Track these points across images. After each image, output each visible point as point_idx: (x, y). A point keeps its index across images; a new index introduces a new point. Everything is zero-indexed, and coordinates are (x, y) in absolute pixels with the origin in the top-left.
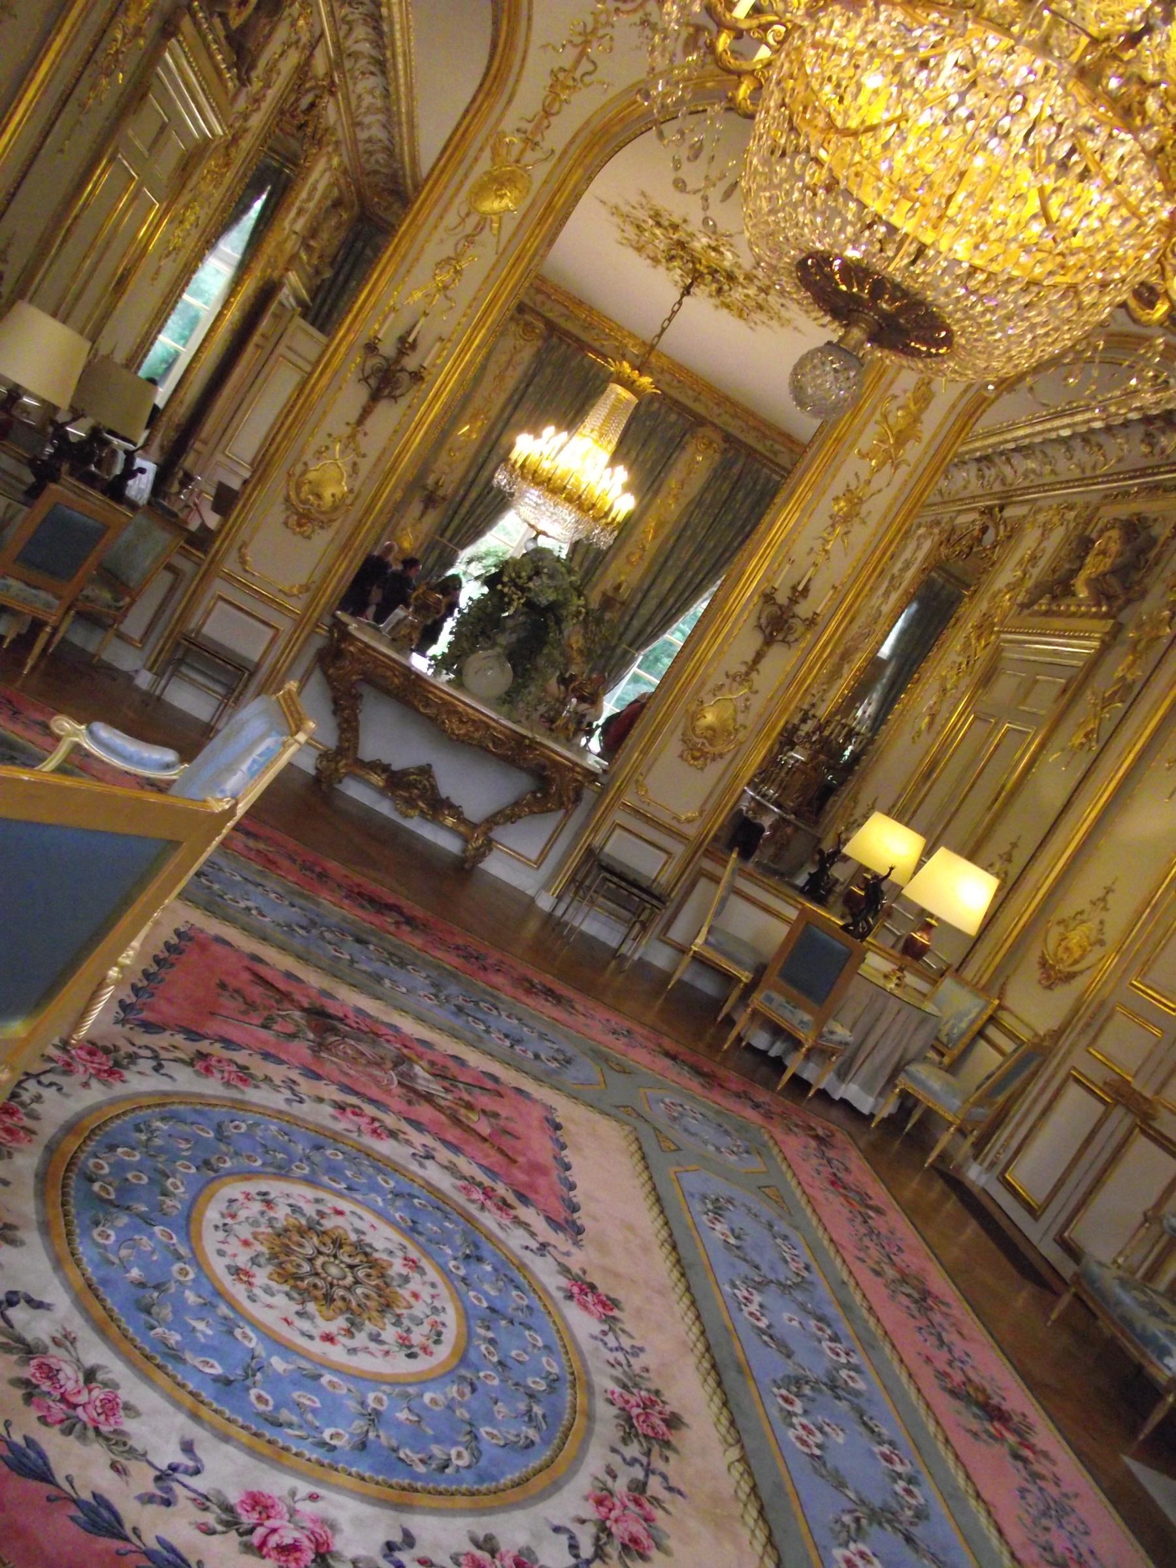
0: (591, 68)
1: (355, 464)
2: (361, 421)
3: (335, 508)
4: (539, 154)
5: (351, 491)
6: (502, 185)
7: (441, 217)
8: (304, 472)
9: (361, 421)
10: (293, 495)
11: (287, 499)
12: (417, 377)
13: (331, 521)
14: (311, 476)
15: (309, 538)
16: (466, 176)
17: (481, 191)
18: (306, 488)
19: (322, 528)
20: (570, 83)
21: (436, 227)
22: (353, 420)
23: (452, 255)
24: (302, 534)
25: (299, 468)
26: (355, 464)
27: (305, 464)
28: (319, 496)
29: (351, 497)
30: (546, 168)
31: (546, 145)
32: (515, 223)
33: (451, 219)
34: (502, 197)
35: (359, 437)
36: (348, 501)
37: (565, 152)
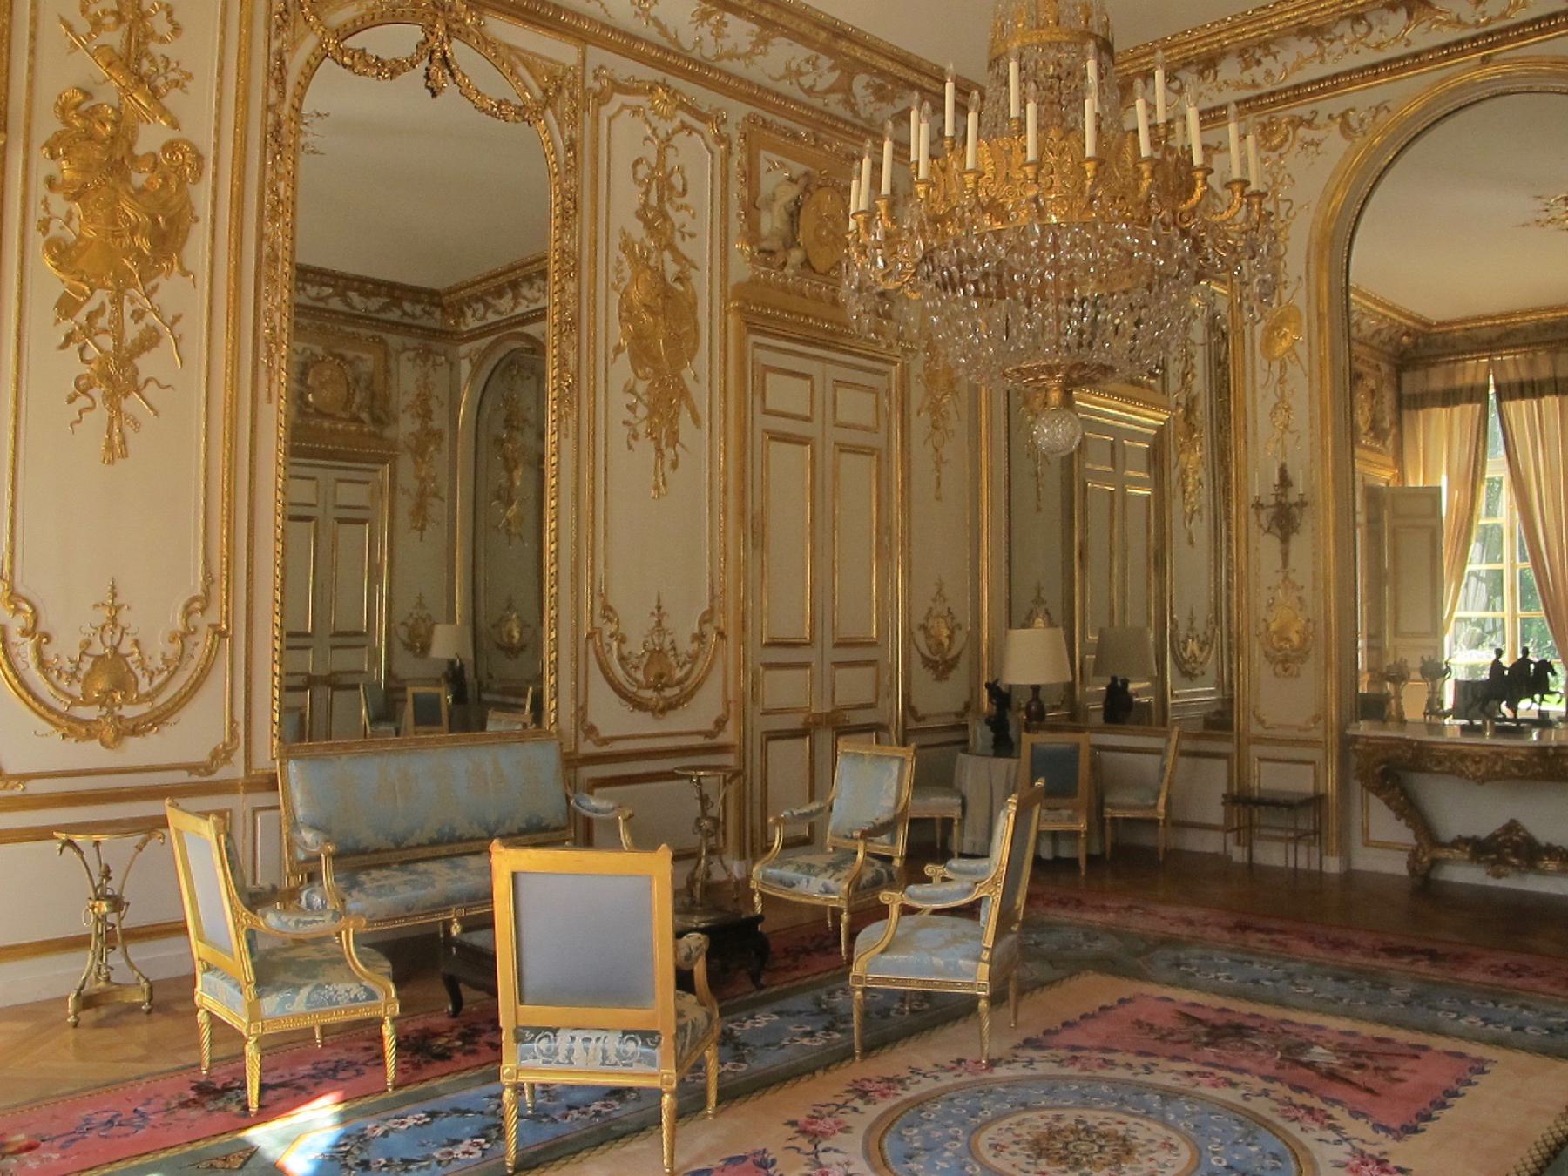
0: (1288, 204)
1: (1300, 598)
2: (1285, 563)
3: (1304, 640)
4: (1291, 288)
5: (1308, 621)
6: (1279, 328)
7: (1253, 382)
8: (1268, 628)
9: (1285, 563)
10: (1268, 648)
11: (1266, 654)
12: (1302, 504)
13: (1307, 653)
14: (1273, 627)
15: (1298, 675)
16: (1253, 342)
17: (1268, 343)
18: (1275, 638)
19: (1303, 662)
20: (1281, 226)
21: (1254, 391)
22: (1279, 565)
23: (1277, 400)
24: (1291, 675)
25: (1262, 627)
26: (1300, 598)
27: (1265, 620)
28: (1288, 640)
29: (1311, 624)
30: (1302, 292)
31: (1293, 278)
32: (1306, 346)
33: (1260, 378)
34: (1285, 335)
35: (1292, 576)
36: (1311, 630)
37: (1308, 272)
